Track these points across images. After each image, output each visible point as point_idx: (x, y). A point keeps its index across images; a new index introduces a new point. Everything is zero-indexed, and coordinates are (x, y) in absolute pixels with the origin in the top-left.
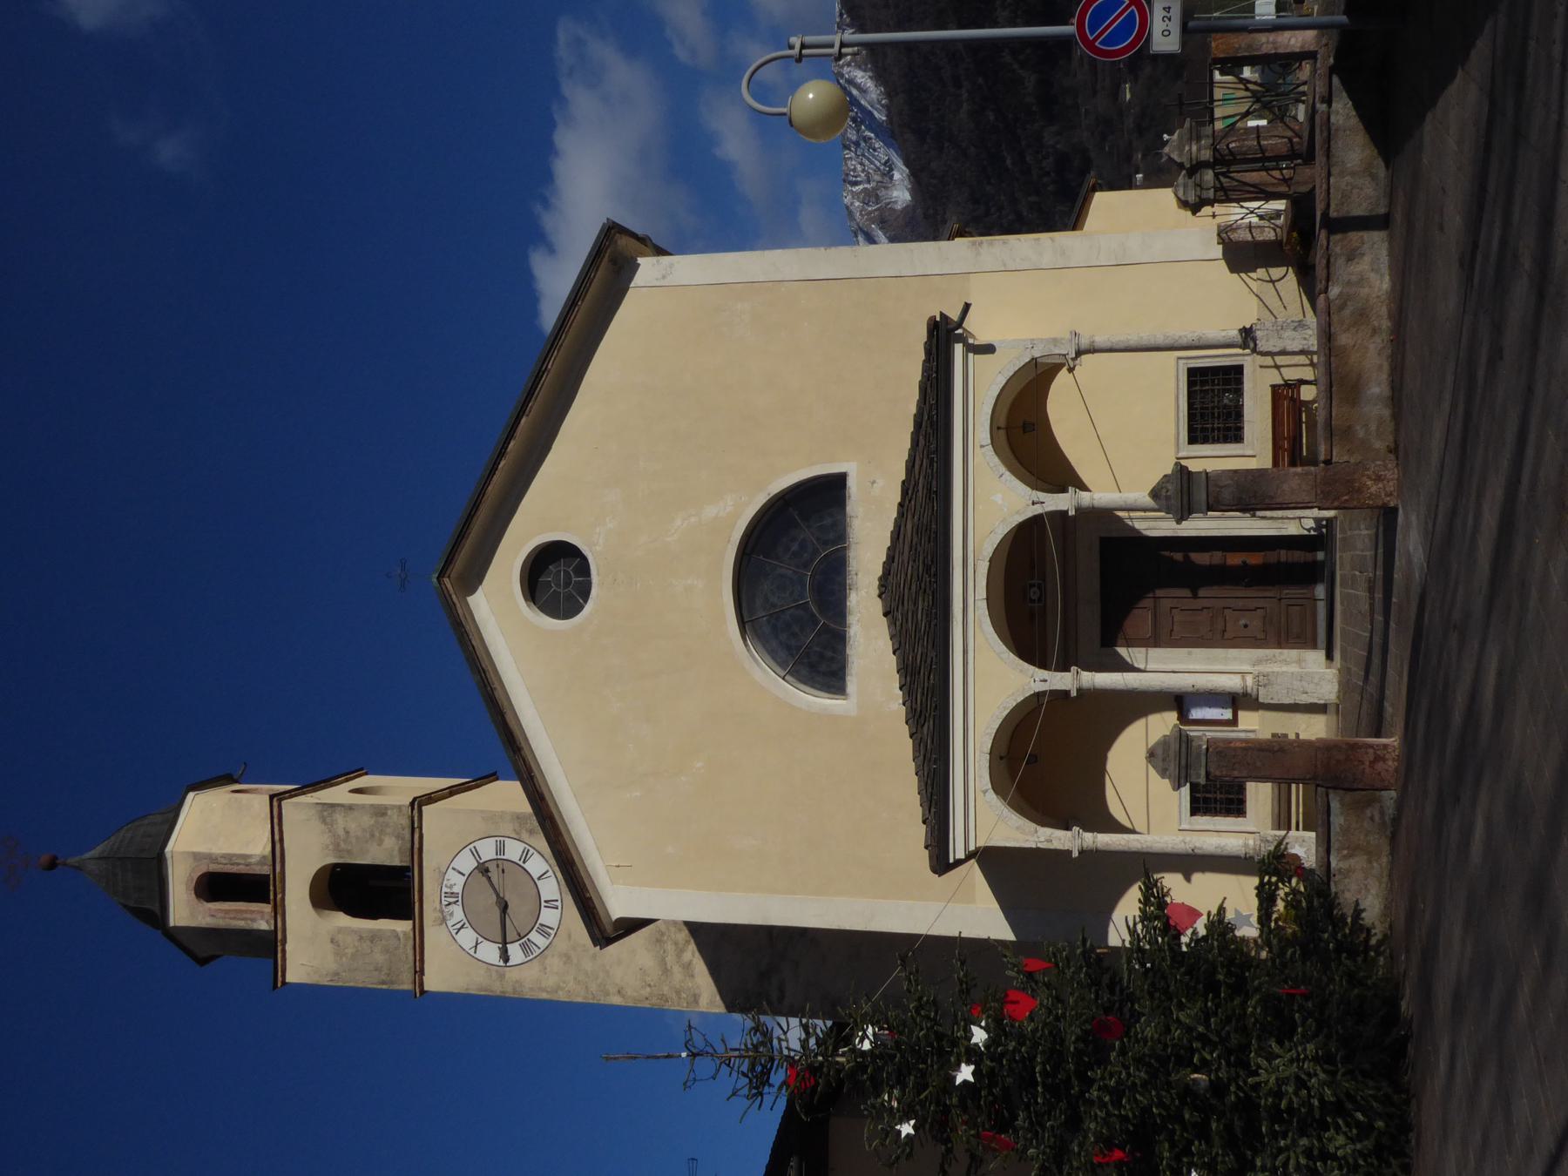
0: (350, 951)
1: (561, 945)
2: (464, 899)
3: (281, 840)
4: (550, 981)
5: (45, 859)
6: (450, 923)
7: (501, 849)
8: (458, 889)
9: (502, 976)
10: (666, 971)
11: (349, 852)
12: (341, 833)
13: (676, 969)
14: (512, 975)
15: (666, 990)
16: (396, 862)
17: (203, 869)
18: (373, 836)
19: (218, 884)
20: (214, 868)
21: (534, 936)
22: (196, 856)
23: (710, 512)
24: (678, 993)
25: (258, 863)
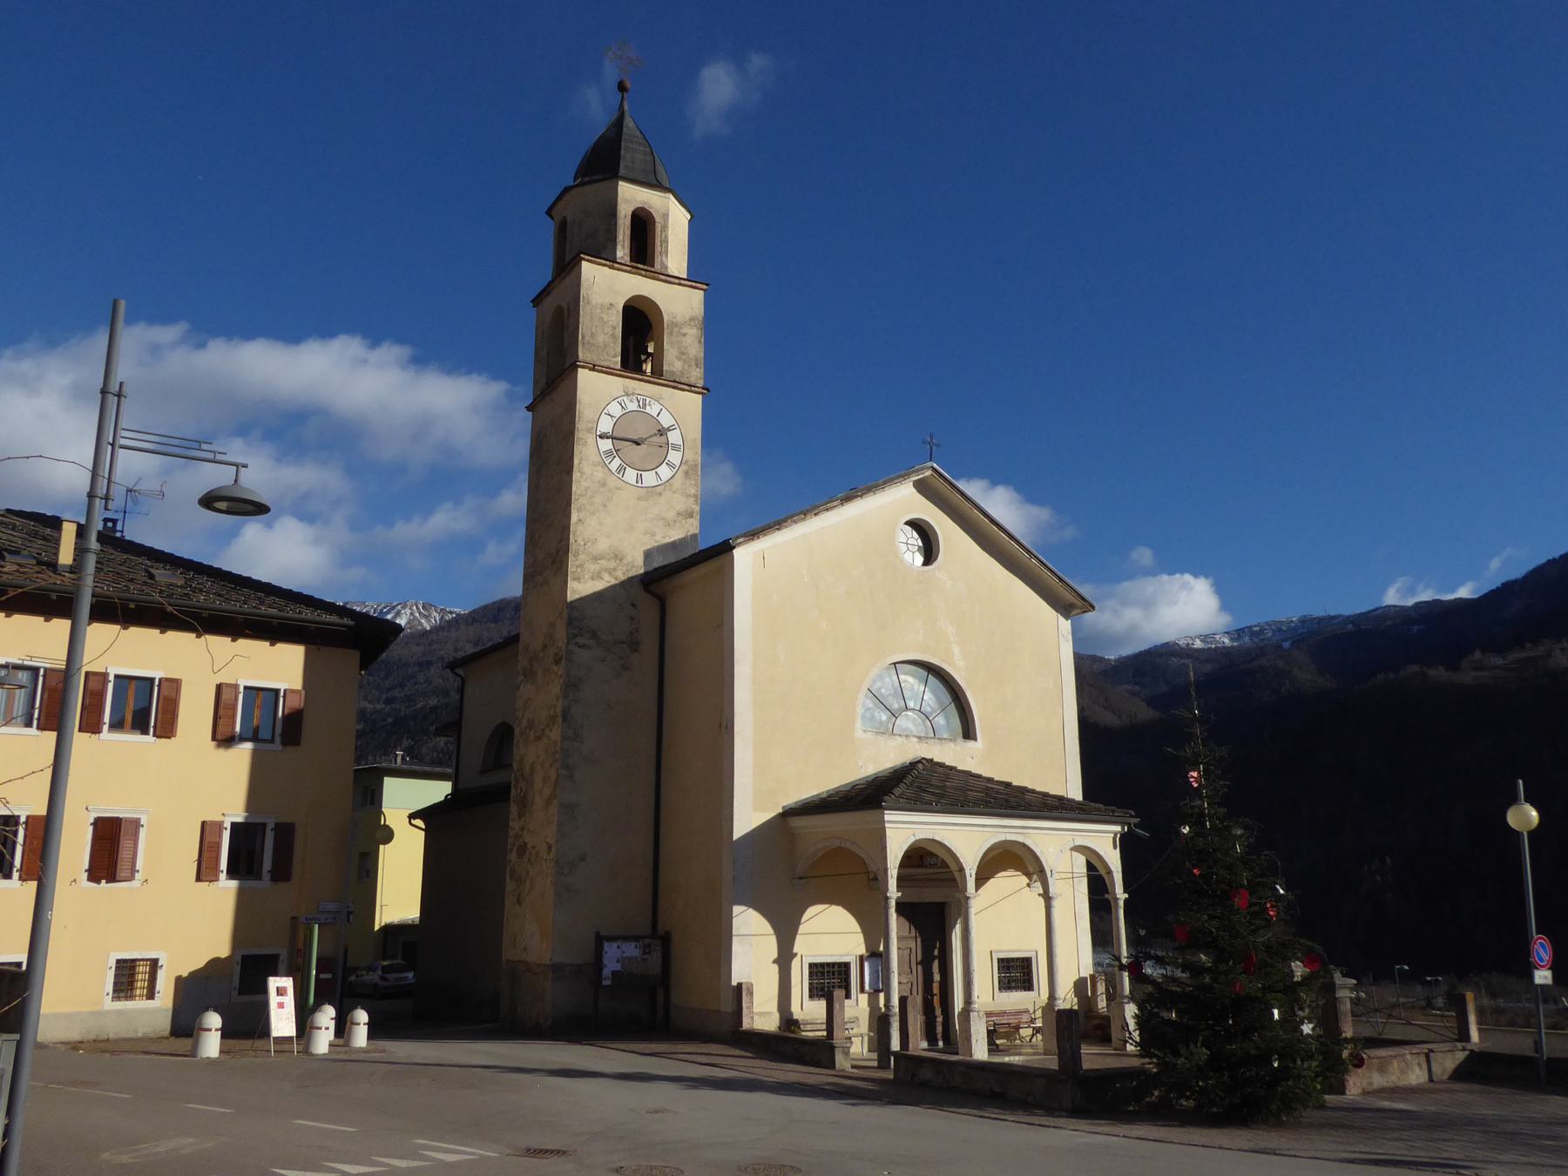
1: (612, 482)
2: (641, 412)
4: (587, 469)
5: (628, 84)
7: (675, 448)
8: (648, 410)
9: (589, 431)
10: (596, 559)
13: (597, 567)
14: (591, 439)
15: (582, 557)
17: (658, 219)
19: (643, 224)
20: (658, 227)
21: (617, 462)
22: (666, 216)
23: (956, 650)
24: (581, 566)
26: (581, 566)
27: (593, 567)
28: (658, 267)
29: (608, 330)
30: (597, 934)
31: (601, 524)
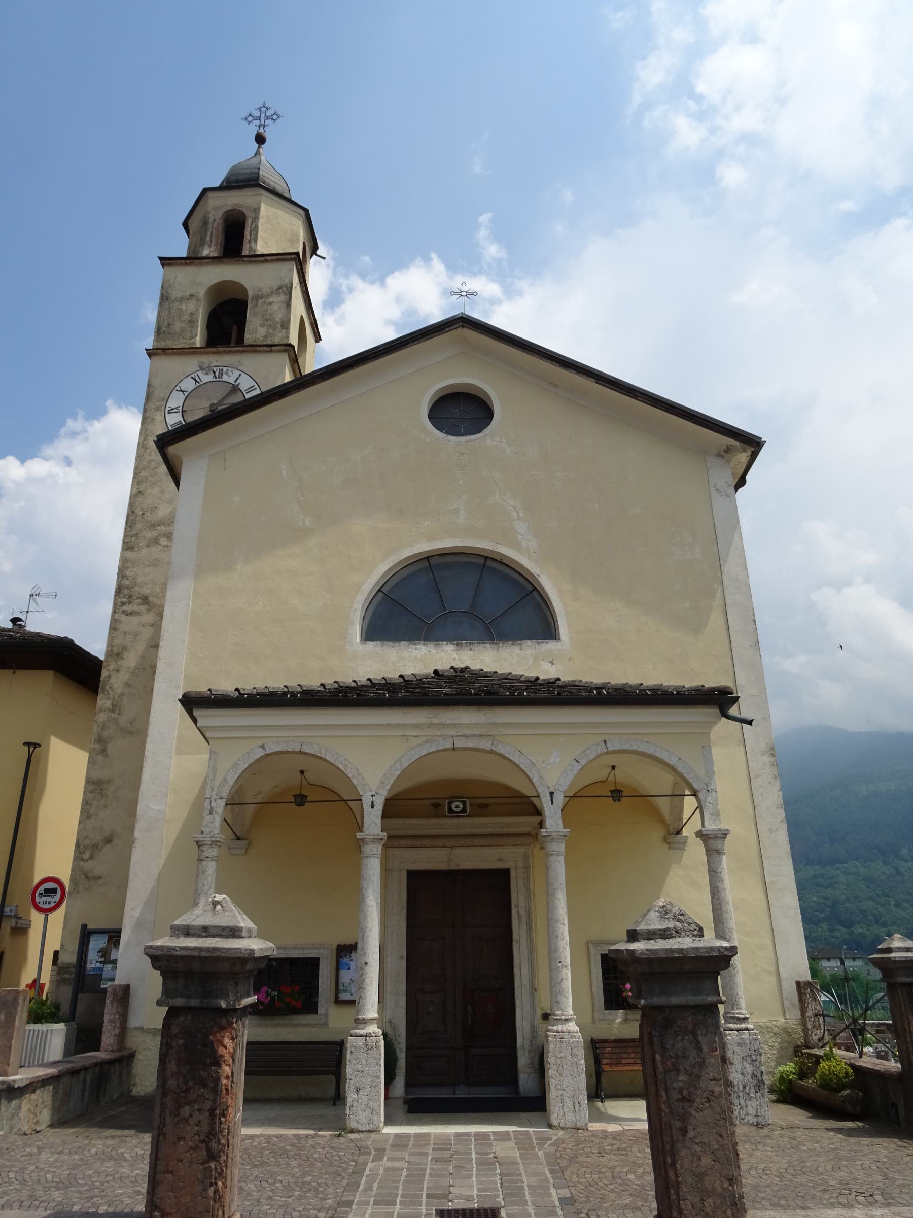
0: (184, 307)
3: (266, 261)
6: (200, 373)
8: (225, 378)
9: (158, 409)
10: (153, 526)
11: (256, 305)
12: (270, 300)
13: (155, 533)
16: (247, 336)
18: (267, 320)
20: (249, 222)
22: (257, 210)
23: (521, 527)
24: (136, 535)
25: (250, 247)
26: (136, 535)
27: (150, 534)
28: (245, 252)
29: (186, 317)
30: (84, 926)
31: (162, 492)
